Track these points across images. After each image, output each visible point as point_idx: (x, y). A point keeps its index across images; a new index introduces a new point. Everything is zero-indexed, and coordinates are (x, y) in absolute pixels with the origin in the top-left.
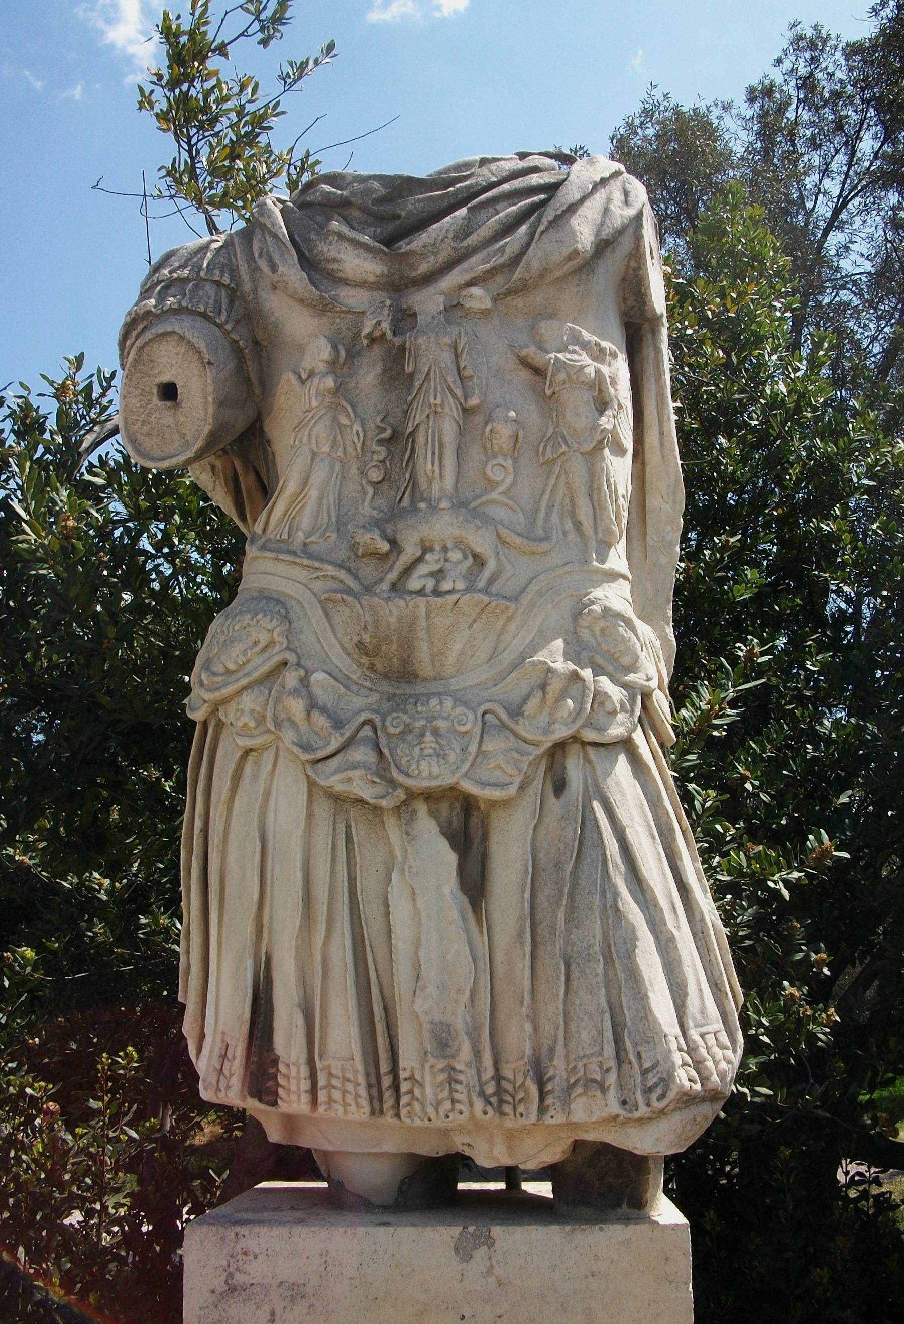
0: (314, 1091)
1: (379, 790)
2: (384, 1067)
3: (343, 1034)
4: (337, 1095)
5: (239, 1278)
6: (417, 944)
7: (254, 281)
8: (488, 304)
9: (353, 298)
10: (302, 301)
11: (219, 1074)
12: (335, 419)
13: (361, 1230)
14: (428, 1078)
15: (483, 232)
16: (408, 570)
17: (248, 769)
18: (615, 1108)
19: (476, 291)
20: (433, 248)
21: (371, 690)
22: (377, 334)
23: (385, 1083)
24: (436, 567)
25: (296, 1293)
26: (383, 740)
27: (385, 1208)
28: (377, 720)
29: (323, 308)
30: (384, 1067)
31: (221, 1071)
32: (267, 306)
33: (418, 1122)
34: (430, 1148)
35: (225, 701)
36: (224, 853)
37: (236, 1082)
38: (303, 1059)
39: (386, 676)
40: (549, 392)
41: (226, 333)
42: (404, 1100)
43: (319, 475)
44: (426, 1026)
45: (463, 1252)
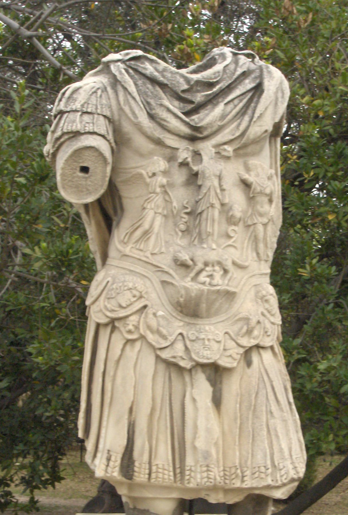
0: (150, 474)
2: (178, 466)
4: (160, 475)
8: (231, 154)
17: (128, 348)
20: (210, 125)
21: (180, 320)
22: (185, 162)
24: (210, 273)
26: (188, 343)
37: (117, 469)
40: (251, 196)
41: (110, 143)
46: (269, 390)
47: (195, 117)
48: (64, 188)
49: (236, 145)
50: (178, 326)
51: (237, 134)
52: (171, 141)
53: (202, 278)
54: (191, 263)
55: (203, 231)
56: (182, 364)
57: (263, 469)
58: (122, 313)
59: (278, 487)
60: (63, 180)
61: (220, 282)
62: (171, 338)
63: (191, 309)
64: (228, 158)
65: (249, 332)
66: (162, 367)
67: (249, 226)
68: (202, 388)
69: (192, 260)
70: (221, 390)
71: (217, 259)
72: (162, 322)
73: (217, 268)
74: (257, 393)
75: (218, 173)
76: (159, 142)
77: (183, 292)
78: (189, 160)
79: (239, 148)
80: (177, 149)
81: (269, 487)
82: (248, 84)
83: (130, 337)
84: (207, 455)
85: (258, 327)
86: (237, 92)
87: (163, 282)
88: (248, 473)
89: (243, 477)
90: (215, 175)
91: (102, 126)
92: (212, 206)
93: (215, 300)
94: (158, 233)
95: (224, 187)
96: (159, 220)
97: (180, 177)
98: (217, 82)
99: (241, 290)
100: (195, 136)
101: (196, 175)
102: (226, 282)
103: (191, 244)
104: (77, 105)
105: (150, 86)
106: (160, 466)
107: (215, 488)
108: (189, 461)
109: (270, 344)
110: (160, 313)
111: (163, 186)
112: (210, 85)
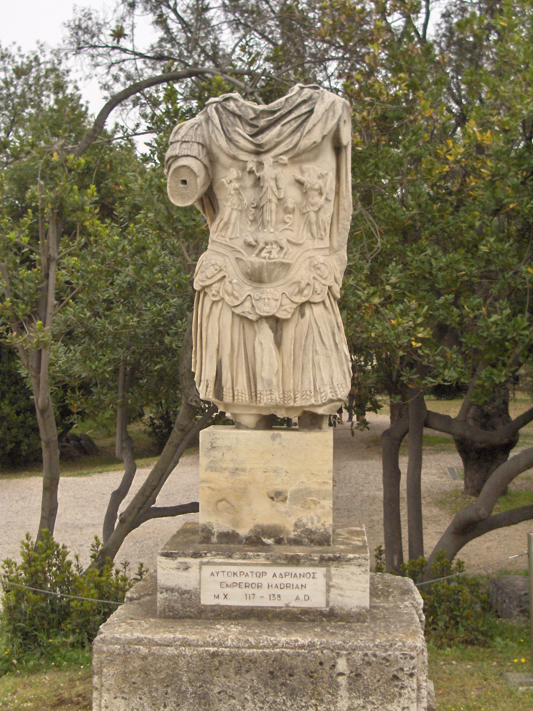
0: (233, 396)
5: (214, 445)
11: (205, 392)
15: (285, 134)
17: (214, 307)
20: (269, 142)
25: (229, 448)
26: (254, 302)
30: (253, 390)
36: (207, 331)
37: (212, 393)
45: (273, 438)
46: (316, 334)
47: (259, 137)
48: (173, 196)
49: (291, 155)
50: (248, 289)
51: (290, 147)
52: (243, 156)
53: (263, 254)
54: (254, 243)
56: (250, 317)
57: (308, 393)
58: (208, 283)
59: (320, 406)
60: (171, 191)
61: (276, 256)
62: (241, 299)
63: (256, 277)
64: (285, 165)
65: (301, 292)
66: (237, 320)
67: (304, 214)
68: (266, 334)
69: (256, 241)
70: (281, 335)
71: (274, 239)
72: (236, 287)
74: (307, 337)
75: (274, 177)
76: (234, 158)
77: (249, 265)
78: (254, 169)
79: (293, 157)
80: (247, 162)
81: (313, 406)
82: (304, 109)
83: (214, 299)
84: (270, 383)
85: (308, 288)
86: (293, 116)
87: (237, 259)
88: (299, 395)
89: (295, 398)
90: (272, 179)
91: (195, 150)
92: (270, 201)
93: (273, 270)
94: (234, 224)
95: (280, 186)
96: (235, 214)
97: (249, 181)
99: (297, 261)
100: (259, 151)
101: (259, 179)
102: (282, 256)
103: (257, 230)
104: (179, 137)
105: (232, 118)
107: (277, 407)
108: (259, 387)
109: (321, 300)
110: (235, 281)
111: (236, 189)
112: (274, 112)
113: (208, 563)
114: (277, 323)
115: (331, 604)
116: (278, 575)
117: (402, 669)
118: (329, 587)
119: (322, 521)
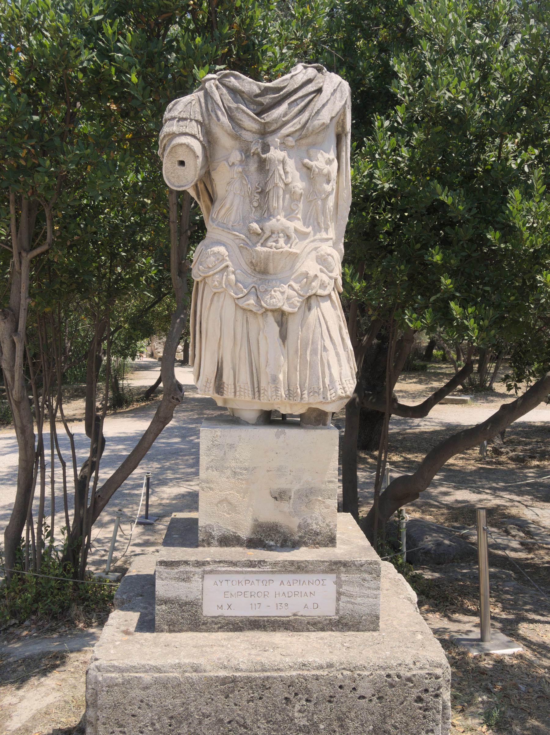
0: (235, 392)
1: (258, 308)
2: (256, 386)
3: (244, 377)
4: (242, 393)
6: (267, 353)
7: (209, 119)
8: (294, 144)
9: (248, 136)
10: (229, 134)
12: (241, 182)
13: (250, 430)
14: (269, 389)
16: (267, 239)
17: (216, 298)
18: (322, 399)
19: (290, 139)
20: (276, 120)
23: (257, 390)
24: (275, 239)
26: (259, 293)
27: (253, 425)
28: (257, 287)
29: (237, 138)
30: (256, 386)
31: (206, 386)
32: (214, 131)
33: (266, 401)
34: (267, 408)
35: (207, 277)
36: (207, 323)
37: (212, 389)
38: (232, 383)
39: (259, 272)
41: (201, 142)
42: (262, 395)
43: (237, 201)
44: (270, 376)
45: (277, 436)
53: (270, 244)
55: (271, 206)
66: (240, 312)
69: (262, 229)
73: (281, 235)
75: (281, 158)
86: (300, 94)
89: (302, 395)
91: (195, 128)
92: (276, 185)
98: (284, 87)
106: (242, 387)
112: (280, 89)
113: (211, 572)
114: (282, 318)
115: (341, 613)
116: (285, 583)
117: (426, 691)
118: (339, 594)
119: (327, 522)
